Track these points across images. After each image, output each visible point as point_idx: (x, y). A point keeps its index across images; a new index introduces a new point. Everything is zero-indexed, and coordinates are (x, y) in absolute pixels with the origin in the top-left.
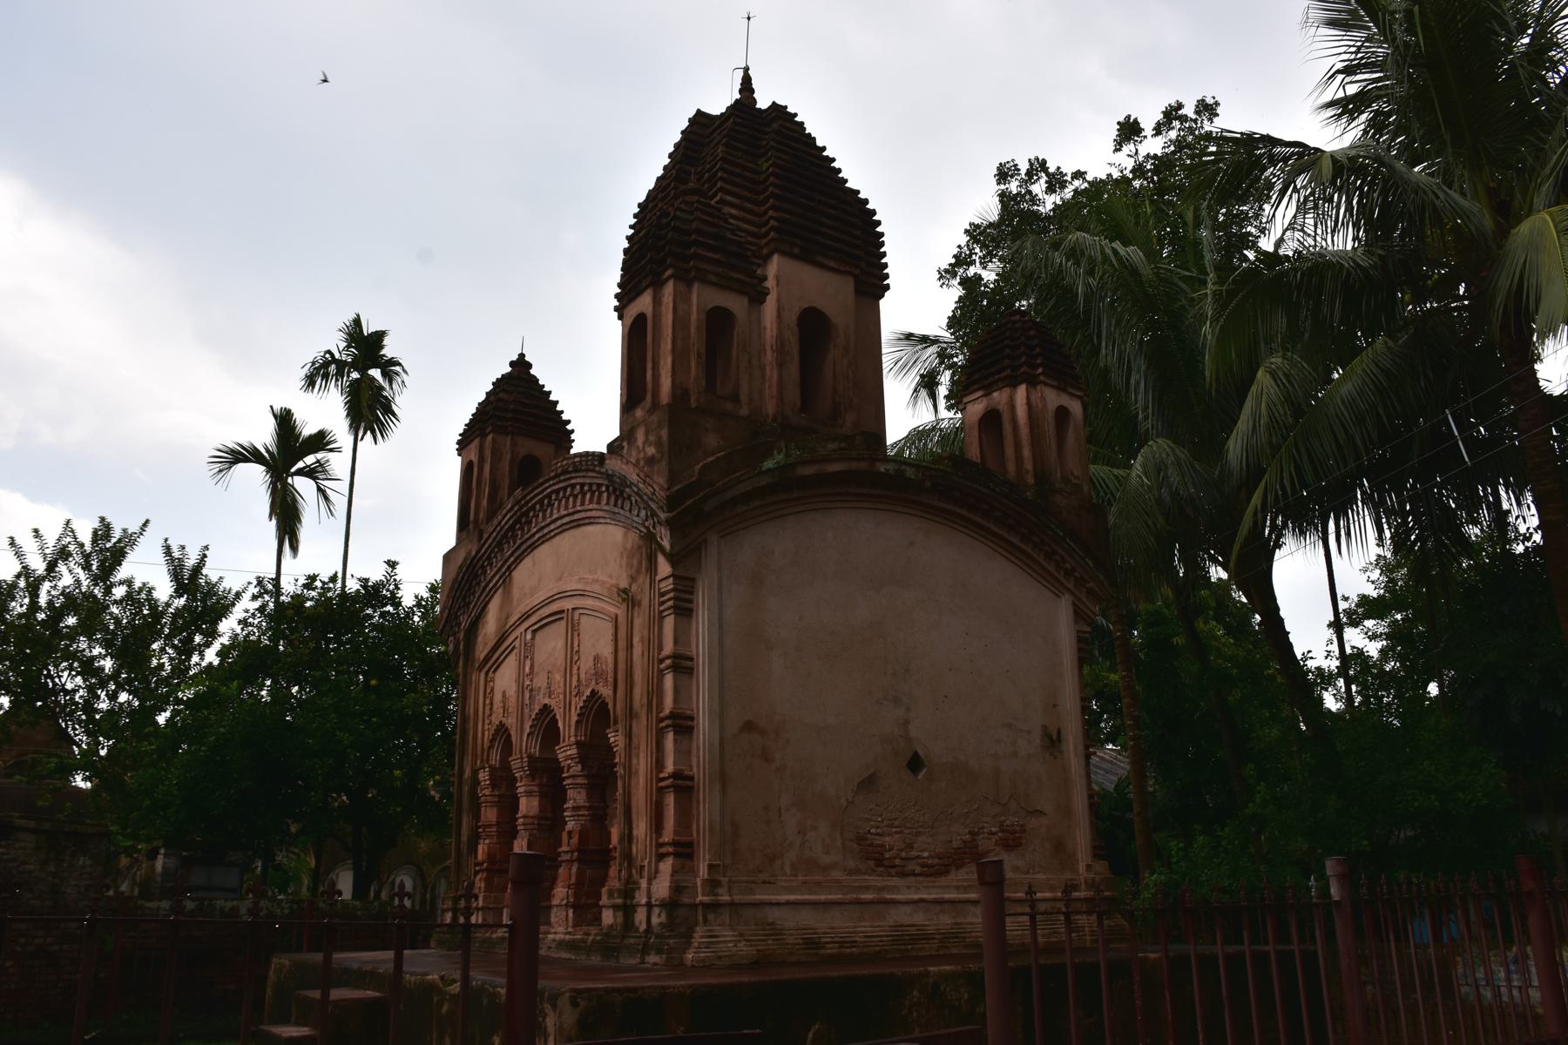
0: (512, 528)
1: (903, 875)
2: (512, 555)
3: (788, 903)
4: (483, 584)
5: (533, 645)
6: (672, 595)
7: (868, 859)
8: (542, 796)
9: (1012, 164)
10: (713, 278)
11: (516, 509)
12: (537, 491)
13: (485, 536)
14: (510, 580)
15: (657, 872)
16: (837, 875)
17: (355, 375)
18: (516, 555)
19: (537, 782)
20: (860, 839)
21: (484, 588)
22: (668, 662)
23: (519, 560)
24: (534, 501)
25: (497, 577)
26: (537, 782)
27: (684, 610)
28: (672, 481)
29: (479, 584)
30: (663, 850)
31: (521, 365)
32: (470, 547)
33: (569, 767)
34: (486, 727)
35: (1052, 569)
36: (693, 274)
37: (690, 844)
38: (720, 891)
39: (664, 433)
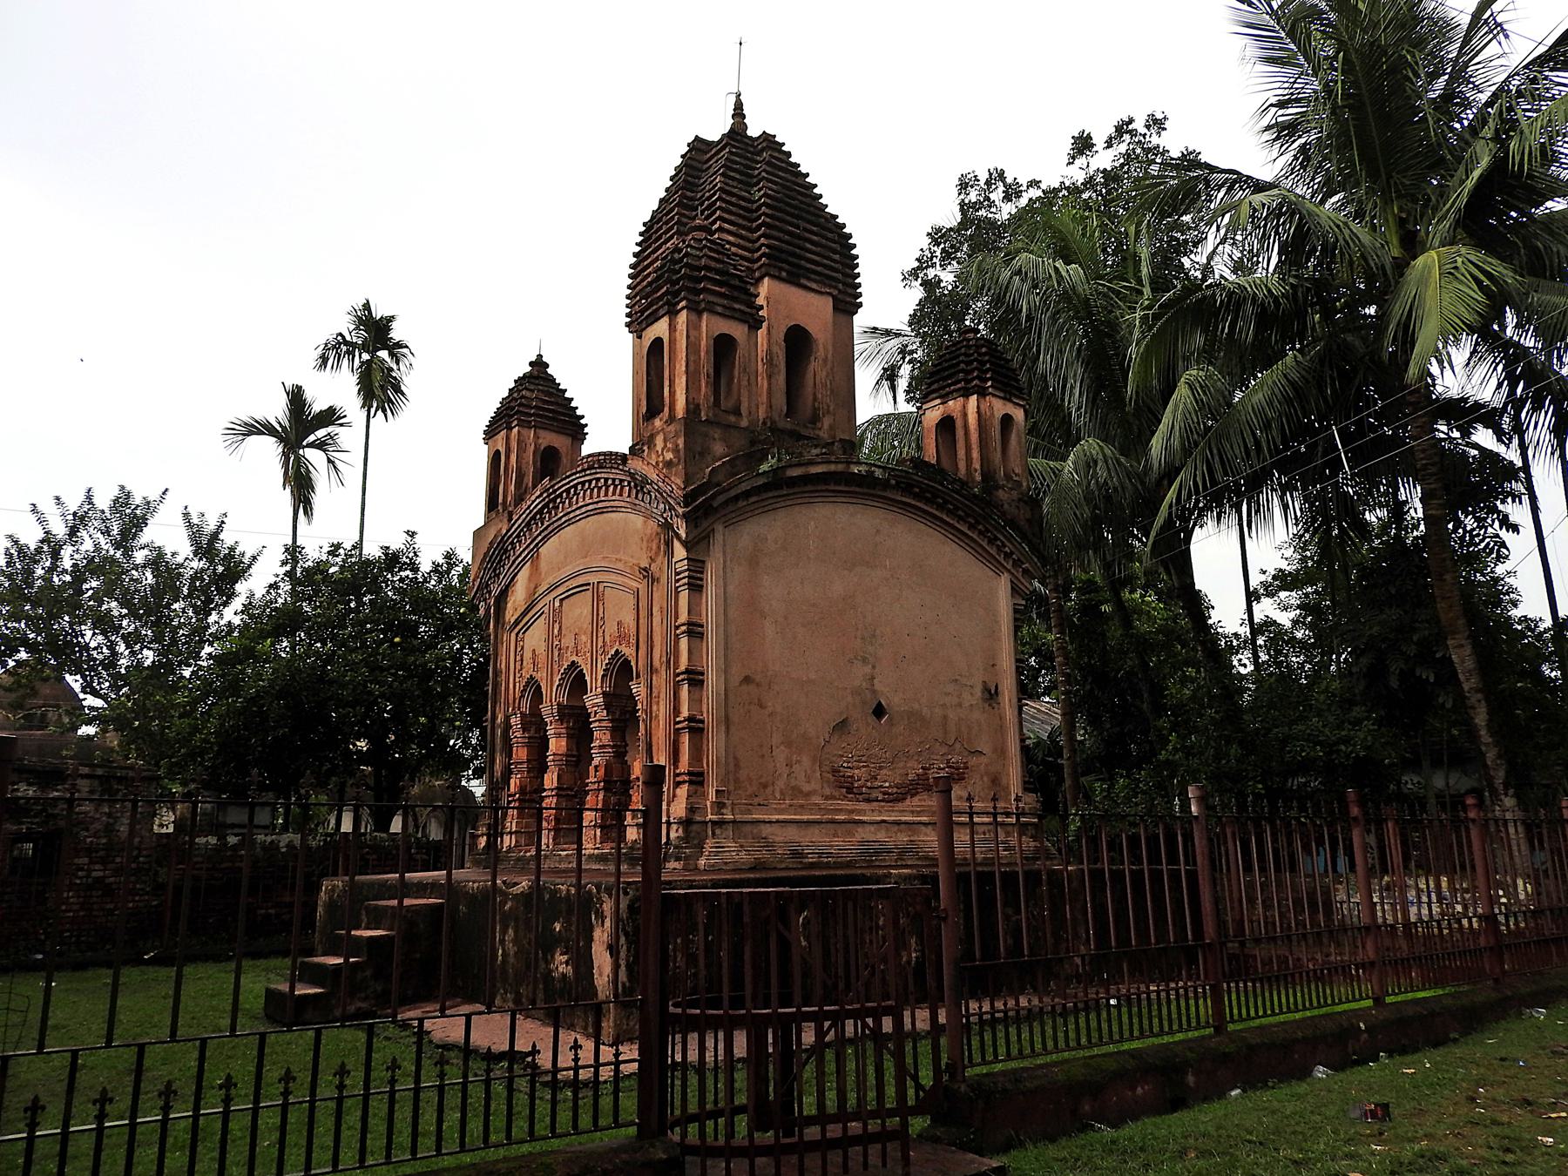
0: (540, 512)
1: (868, 801)
2: (539, 534)
3: (778, 821)
4: (512, 559)
5: (561, 611)
6: (686, 574)
7: (841, 787)
8: (569, 737)
9: (972, 175)
10: (719, 309)
12: (564, 482)
13: (515, 517)
14: (537, 558)
15: (674, 796)
16: (817, 800)
17: (366, 356)
18: (543, 535)
19: (565, 725)
20: (835, 771)
21: (514, 562)
22: (684, 628)
23: (546, 539)
26: (565, 725)
27: (696, 587)
28: (687, 482)
29: (508, 558)
30: (678, 779)
31: (539, 365)
33: (596, 713)
34: (517, 680)
35: (993, 551)
36: (703, 305)
37: (701, 774)
38: (724, 811)
39: (681, 442)
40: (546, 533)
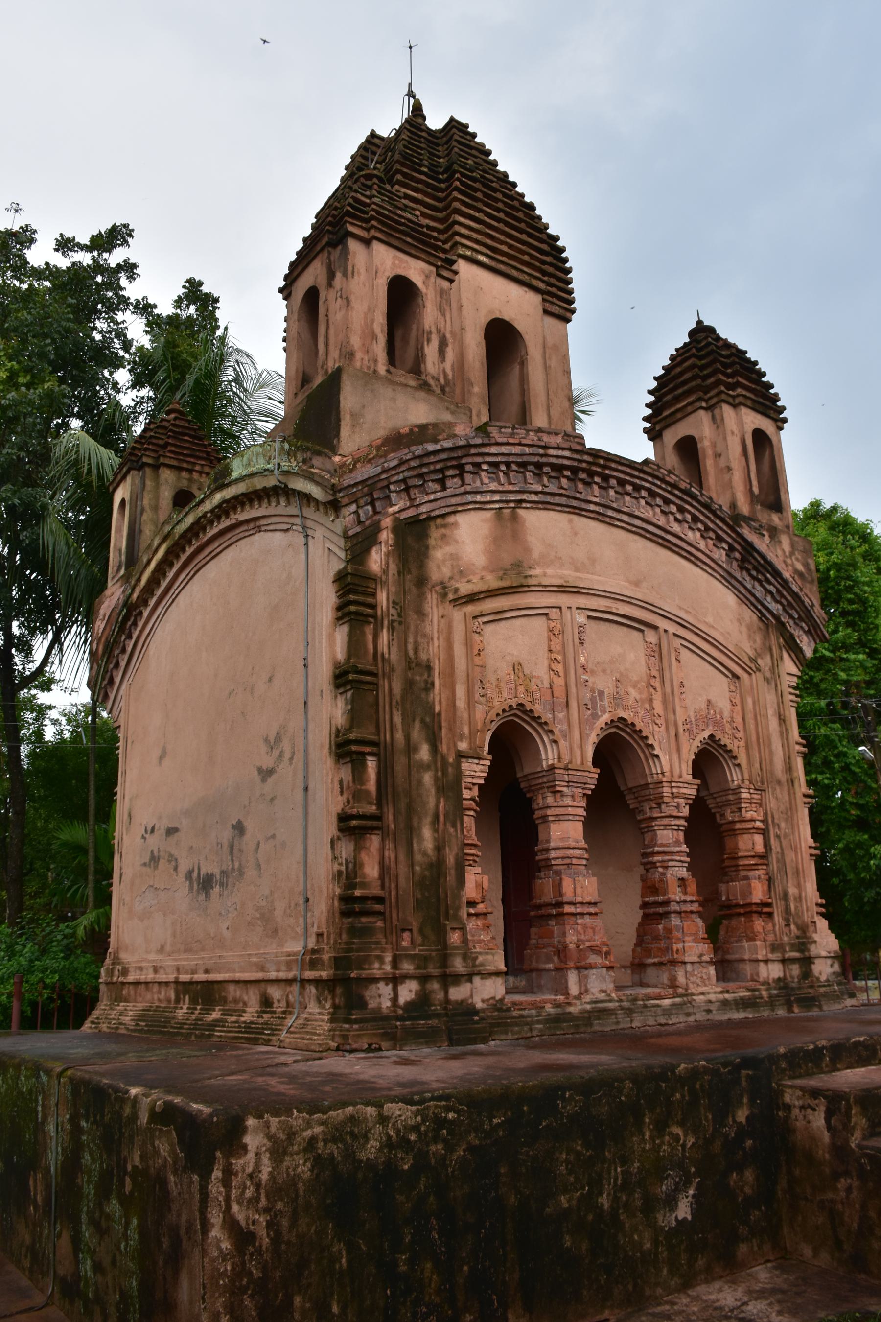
11: (586, 457)
12: (629, 470)
24: (616, 474)
25: (497, 497)
32: (447, 417)
40: (548, 499)
